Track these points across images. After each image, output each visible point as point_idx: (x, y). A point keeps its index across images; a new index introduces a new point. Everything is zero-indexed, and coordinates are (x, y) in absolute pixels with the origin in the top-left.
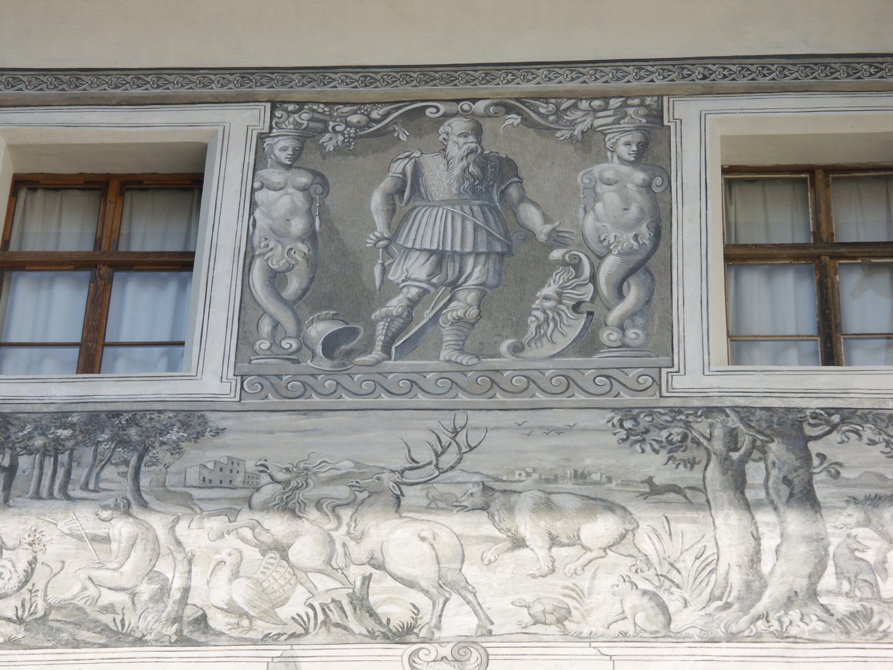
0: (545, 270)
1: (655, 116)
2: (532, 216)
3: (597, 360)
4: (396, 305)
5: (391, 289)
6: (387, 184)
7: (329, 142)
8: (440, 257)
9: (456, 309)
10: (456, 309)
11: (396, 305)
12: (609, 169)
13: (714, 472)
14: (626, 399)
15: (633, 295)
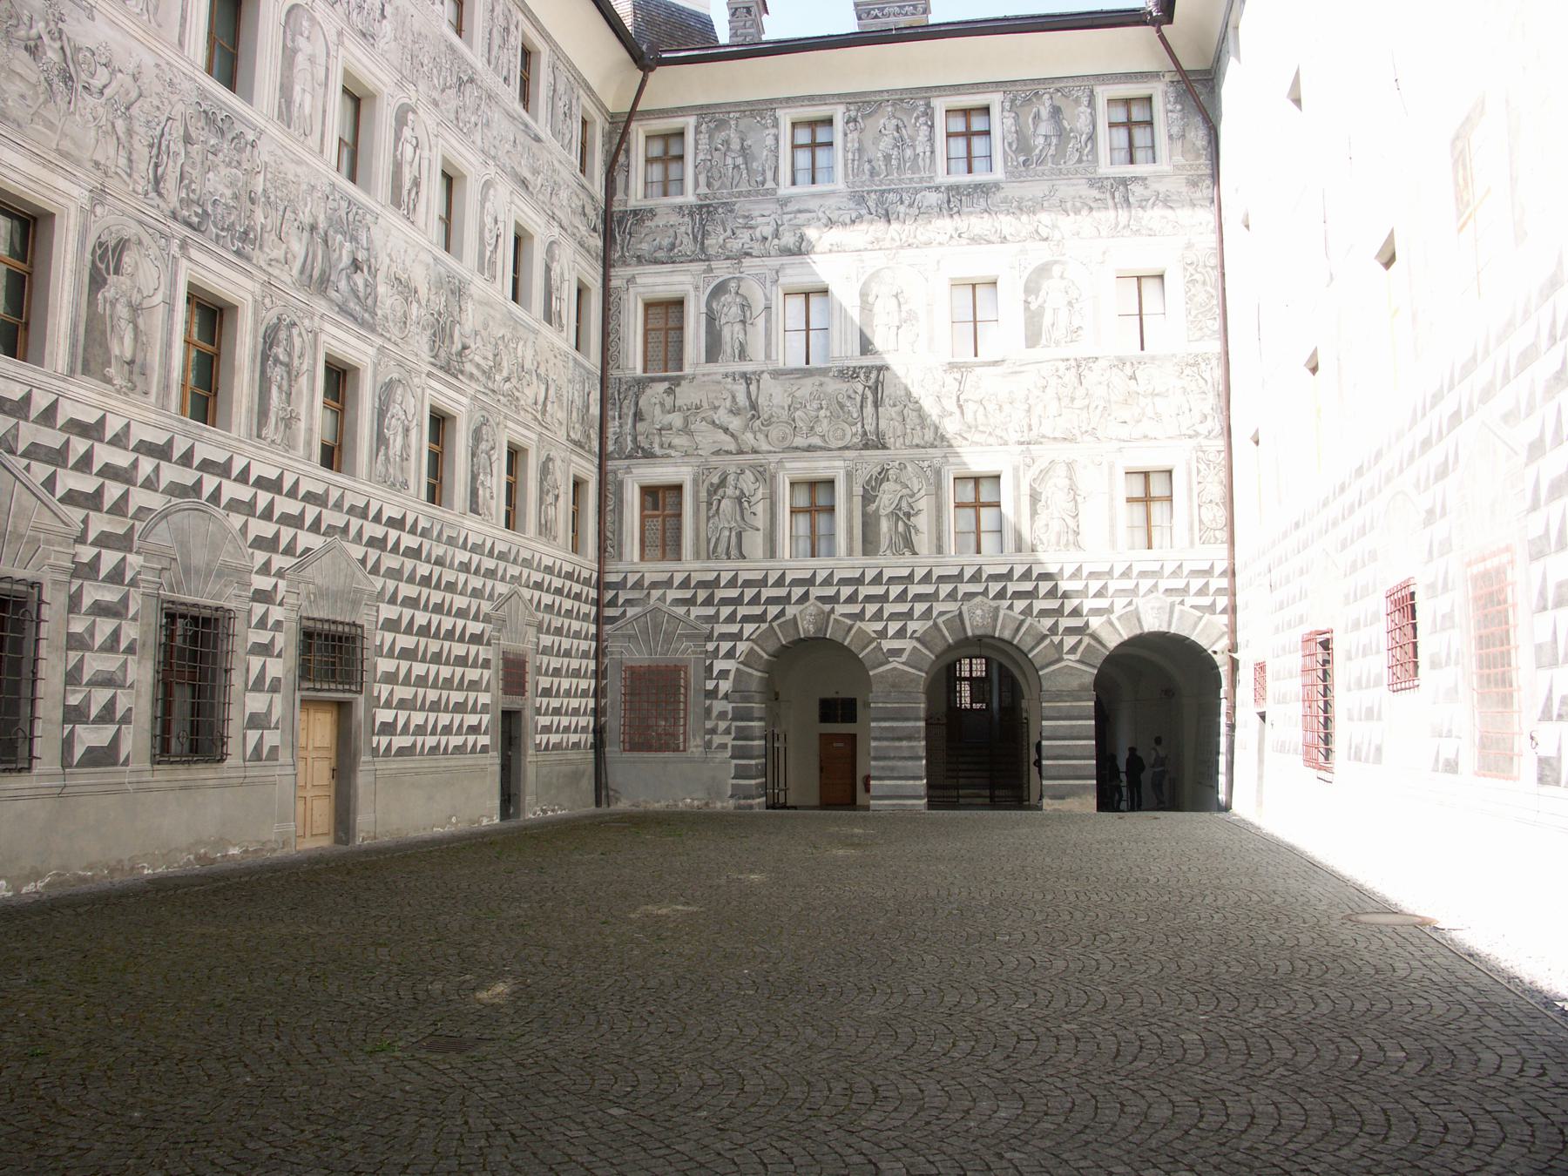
0: (1069, 139)
1: (1092, 92)
2: (1065, 123)
3: (1083, 165)
4: (1037, 151)
5: (1036, 147)
6: (1032, 115)
7: (1018, 103)
8: (1046, 136)
9: (1051, 152)
10: (1051, 152)
11: (1037, 151)
12: (1082, 109)
13: (1108, 195)
14: (1089, 176)
15: (1089, 145)
